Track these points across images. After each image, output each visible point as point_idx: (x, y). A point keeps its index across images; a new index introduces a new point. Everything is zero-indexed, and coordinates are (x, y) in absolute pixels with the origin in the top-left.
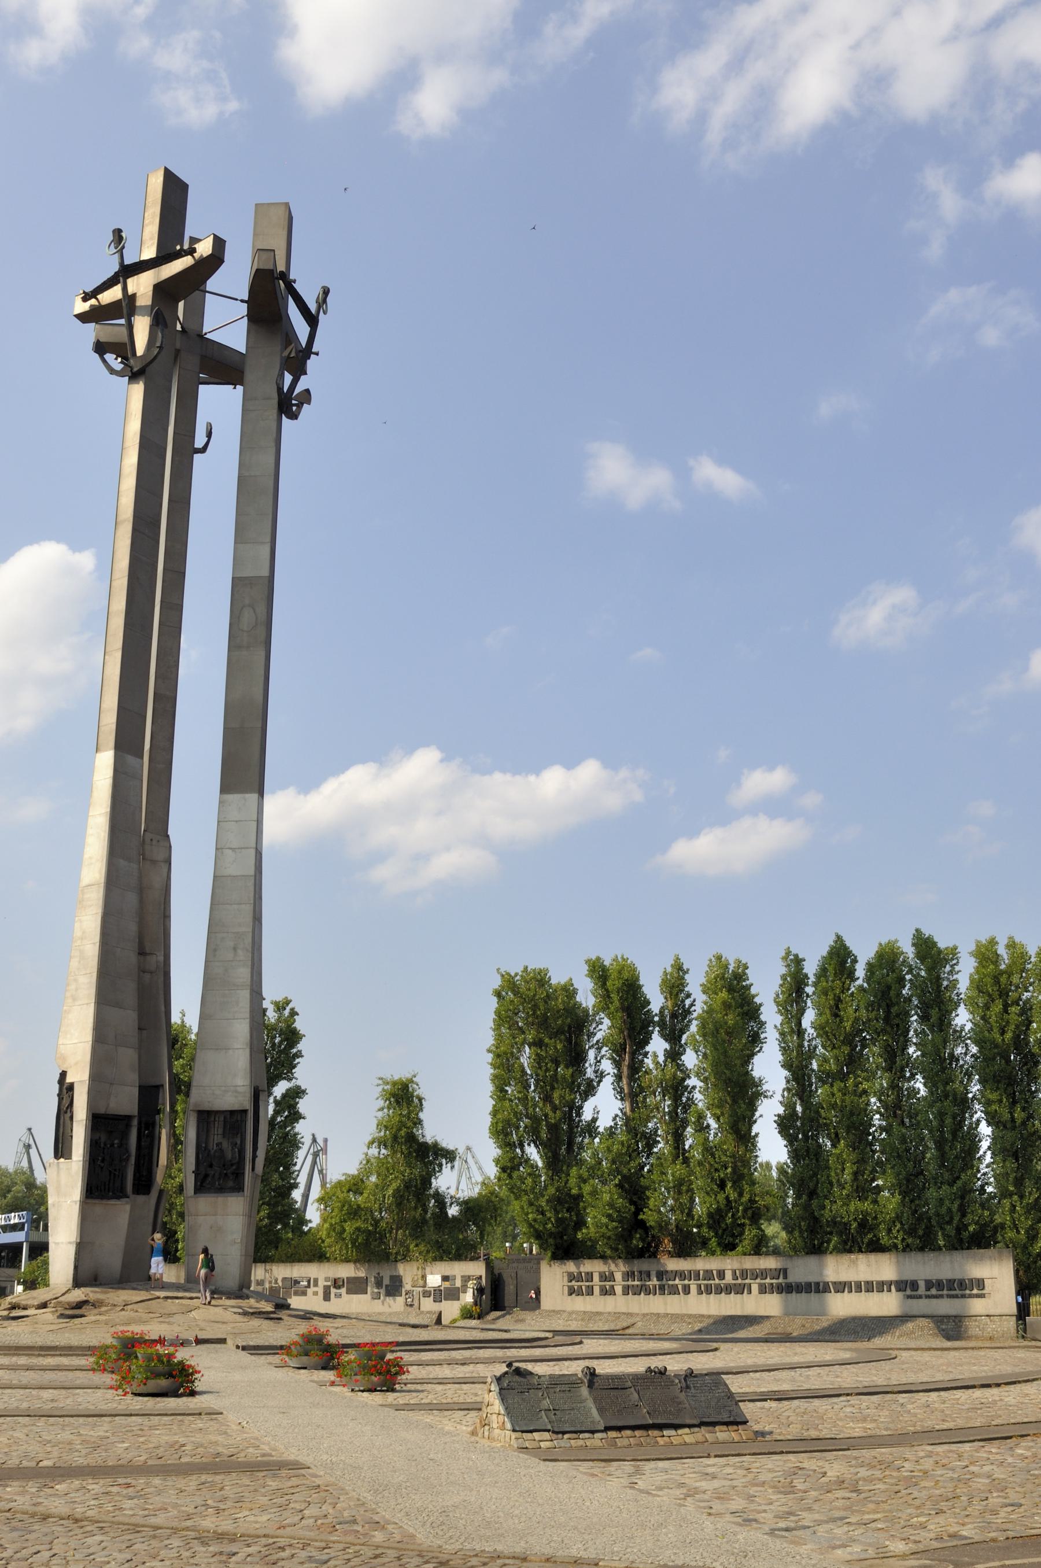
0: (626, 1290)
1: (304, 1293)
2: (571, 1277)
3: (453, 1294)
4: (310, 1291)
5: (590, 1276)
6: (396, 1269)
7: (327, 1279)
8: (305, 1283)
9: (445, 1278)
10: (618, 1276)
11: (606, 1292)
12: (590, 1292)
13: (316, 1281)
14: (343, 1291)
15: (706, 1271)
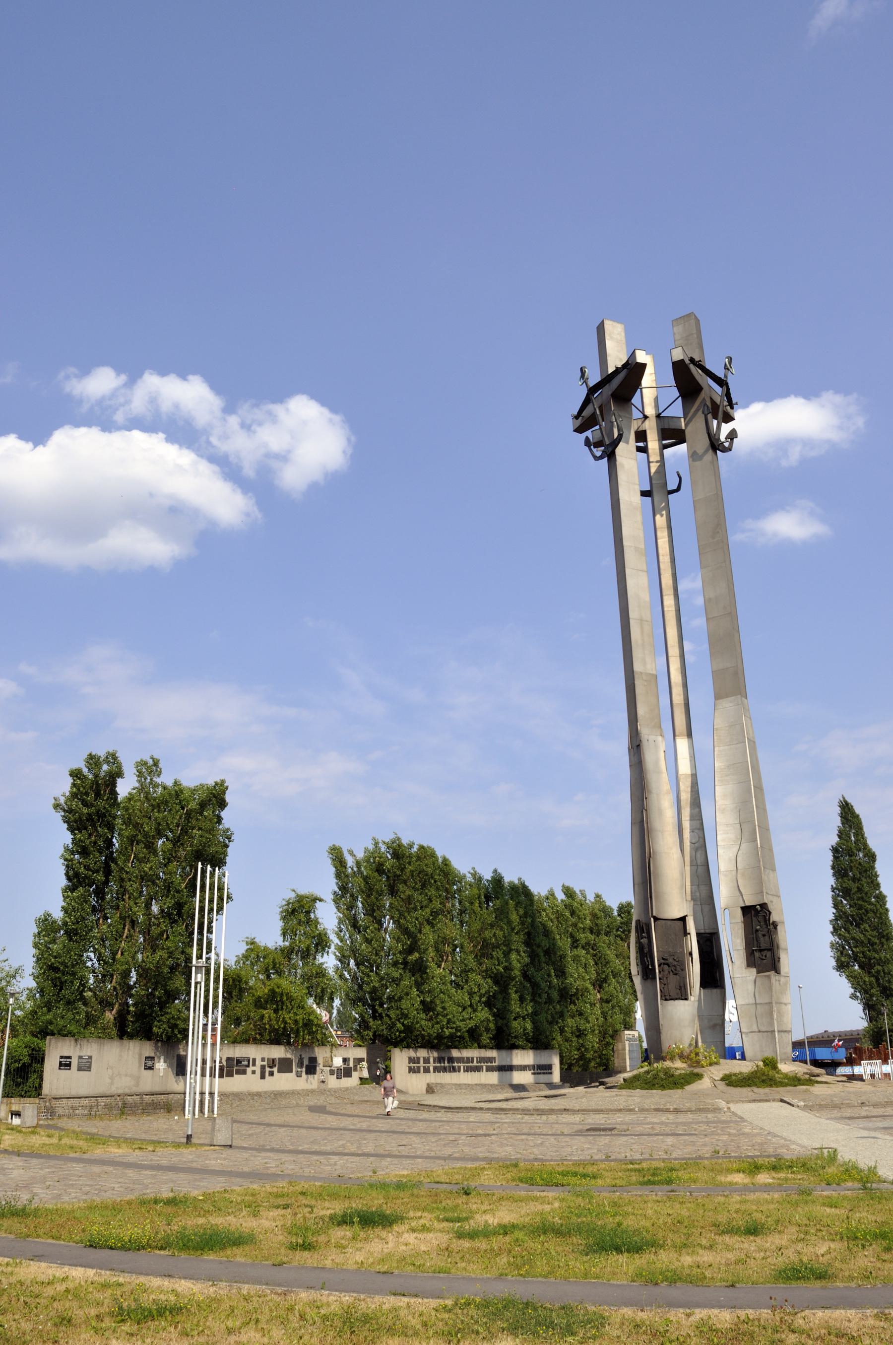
0: (434, 1072)
1: (244, 1072)
2: (411, 1060)
3: (347, 1073)
4: (249, 1070)
5: (419, 1058)
6: (313, 1051)
7: (263, 1059)
8: (246, 1063)
9: (345, 1060)
10: (431, 1060)
11: (427, 1070)
12: (419, 1072)
13: (254, 1060)
14: (275, 1070)
15: (468, 1058)
